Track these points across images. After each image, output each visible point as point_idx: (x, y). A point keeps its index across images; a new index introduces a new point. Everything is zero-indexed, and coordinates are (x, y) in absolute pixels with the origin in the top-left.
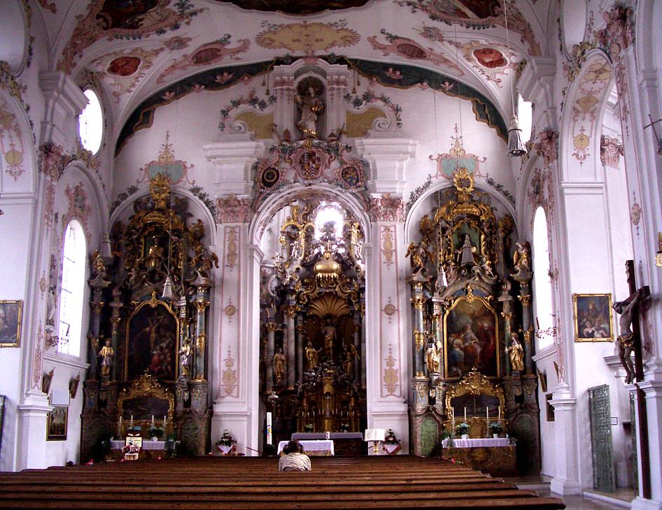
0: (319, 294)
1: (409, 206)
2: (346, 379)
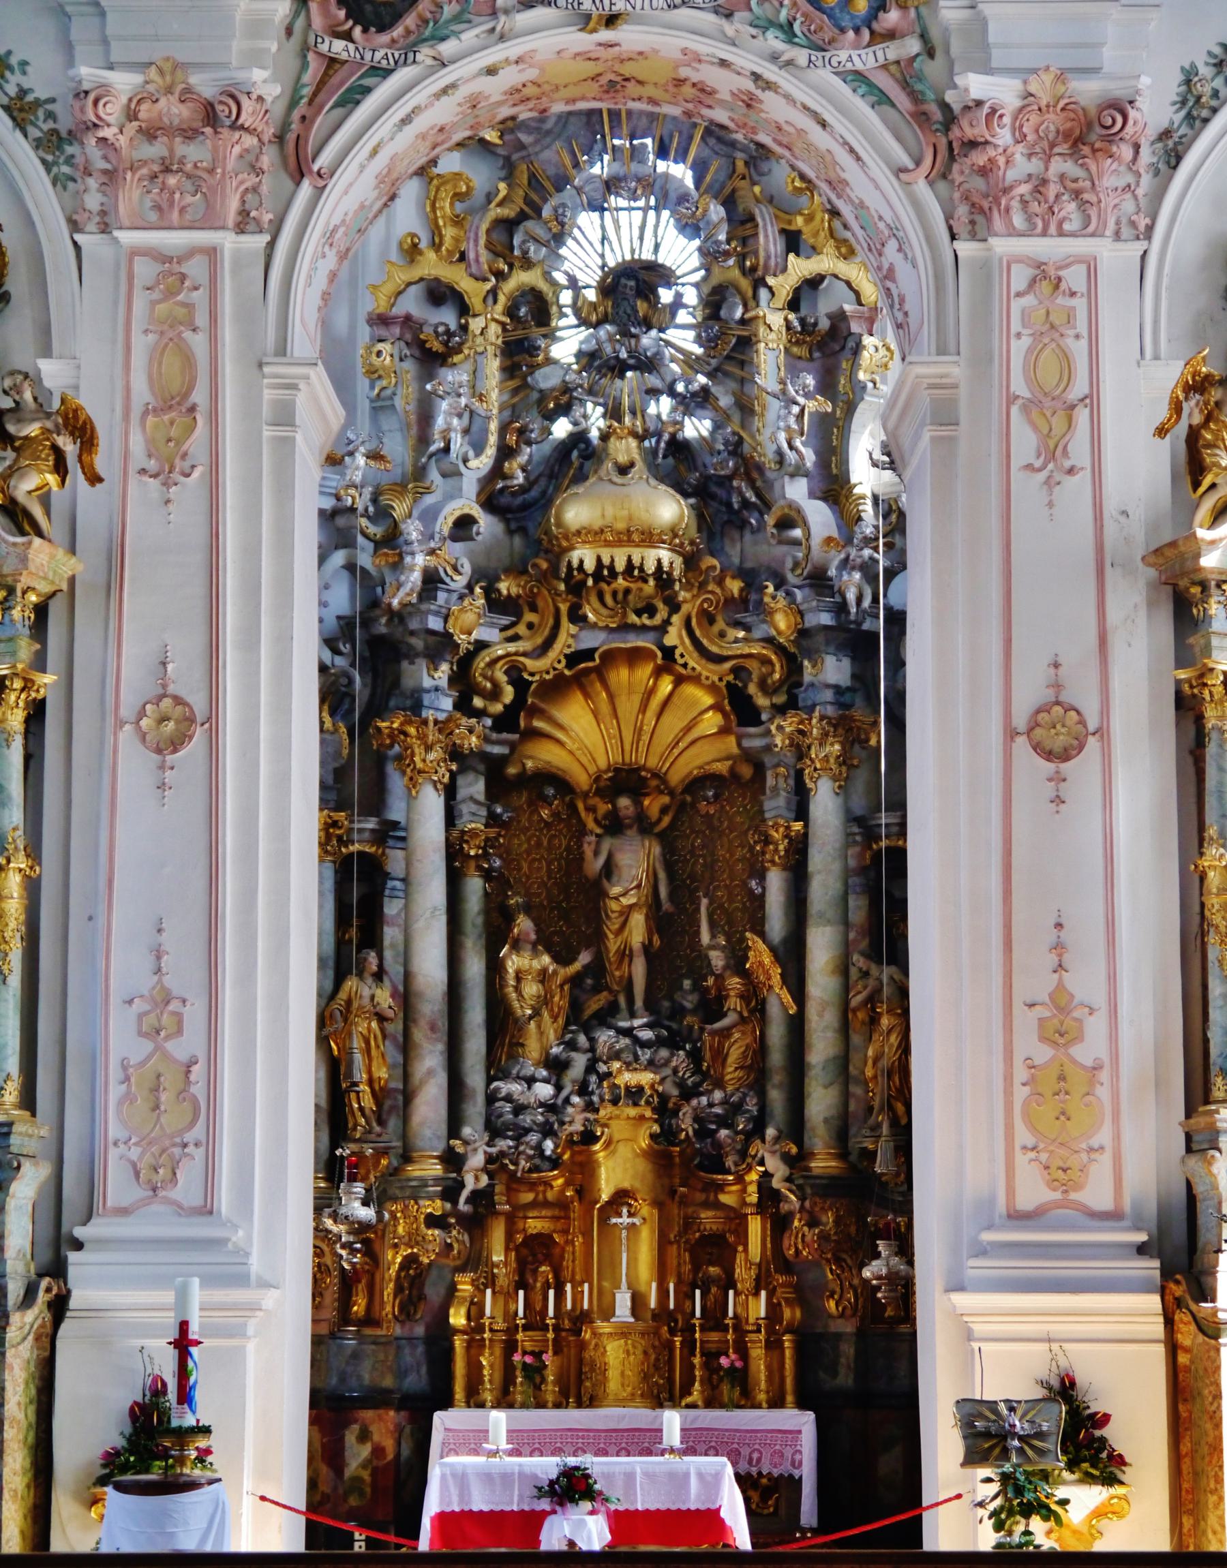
0: (573, 659)
1: (1174, 158)
2: (725, 1121)
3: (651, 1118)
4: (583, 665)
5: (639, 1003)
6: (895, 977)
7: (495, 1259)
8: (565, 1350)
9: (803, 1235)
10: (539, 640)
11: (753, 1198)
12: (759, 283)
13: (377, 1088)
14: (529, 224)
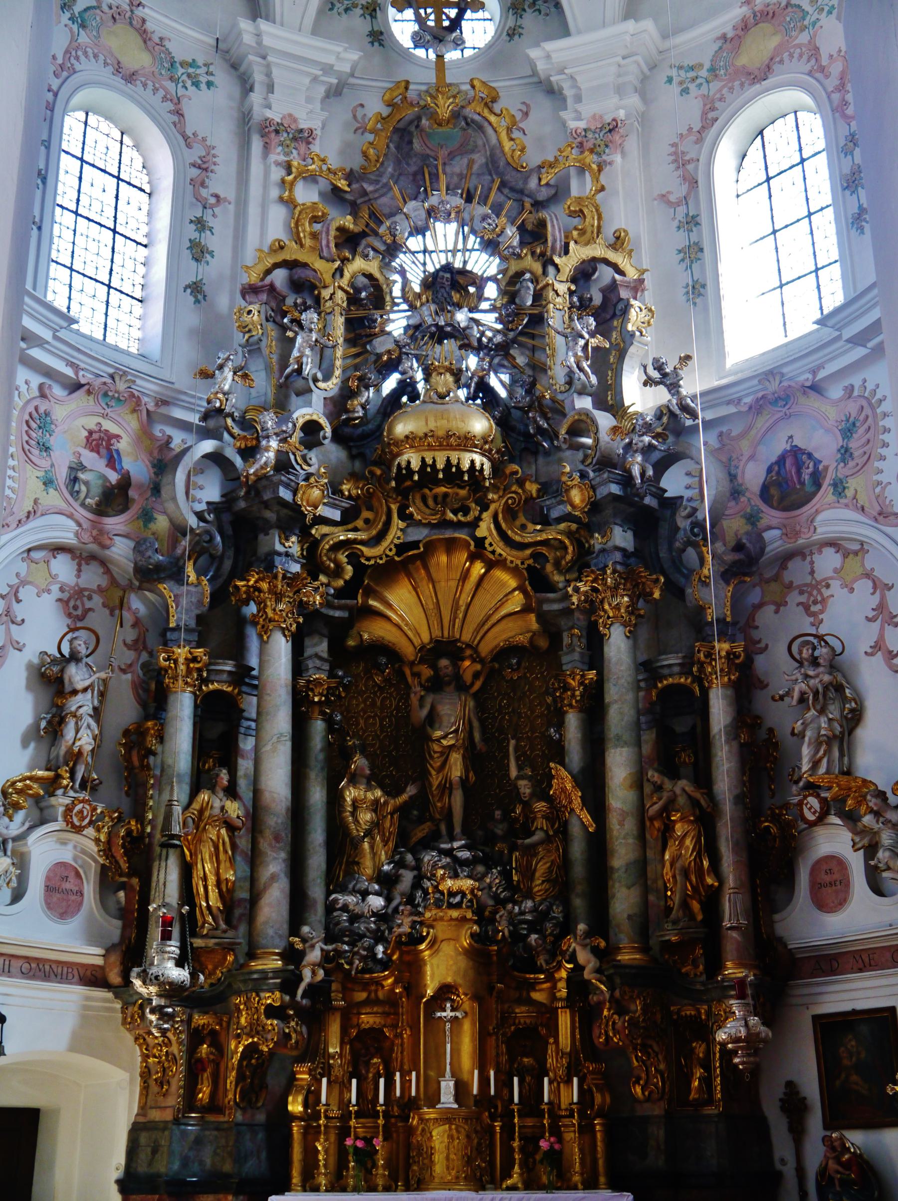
0: (402, 548)
2: (534, 927)
3: (470, 920)
5: (458, 830)
6: (687, 788)
7: (331, 1050)
8: (395, 1135)
9: (614, 1023)
10: (374, 532)
11: (563, 993)
12: (547, 262)
13: (224, 889)
14: (371, 240)
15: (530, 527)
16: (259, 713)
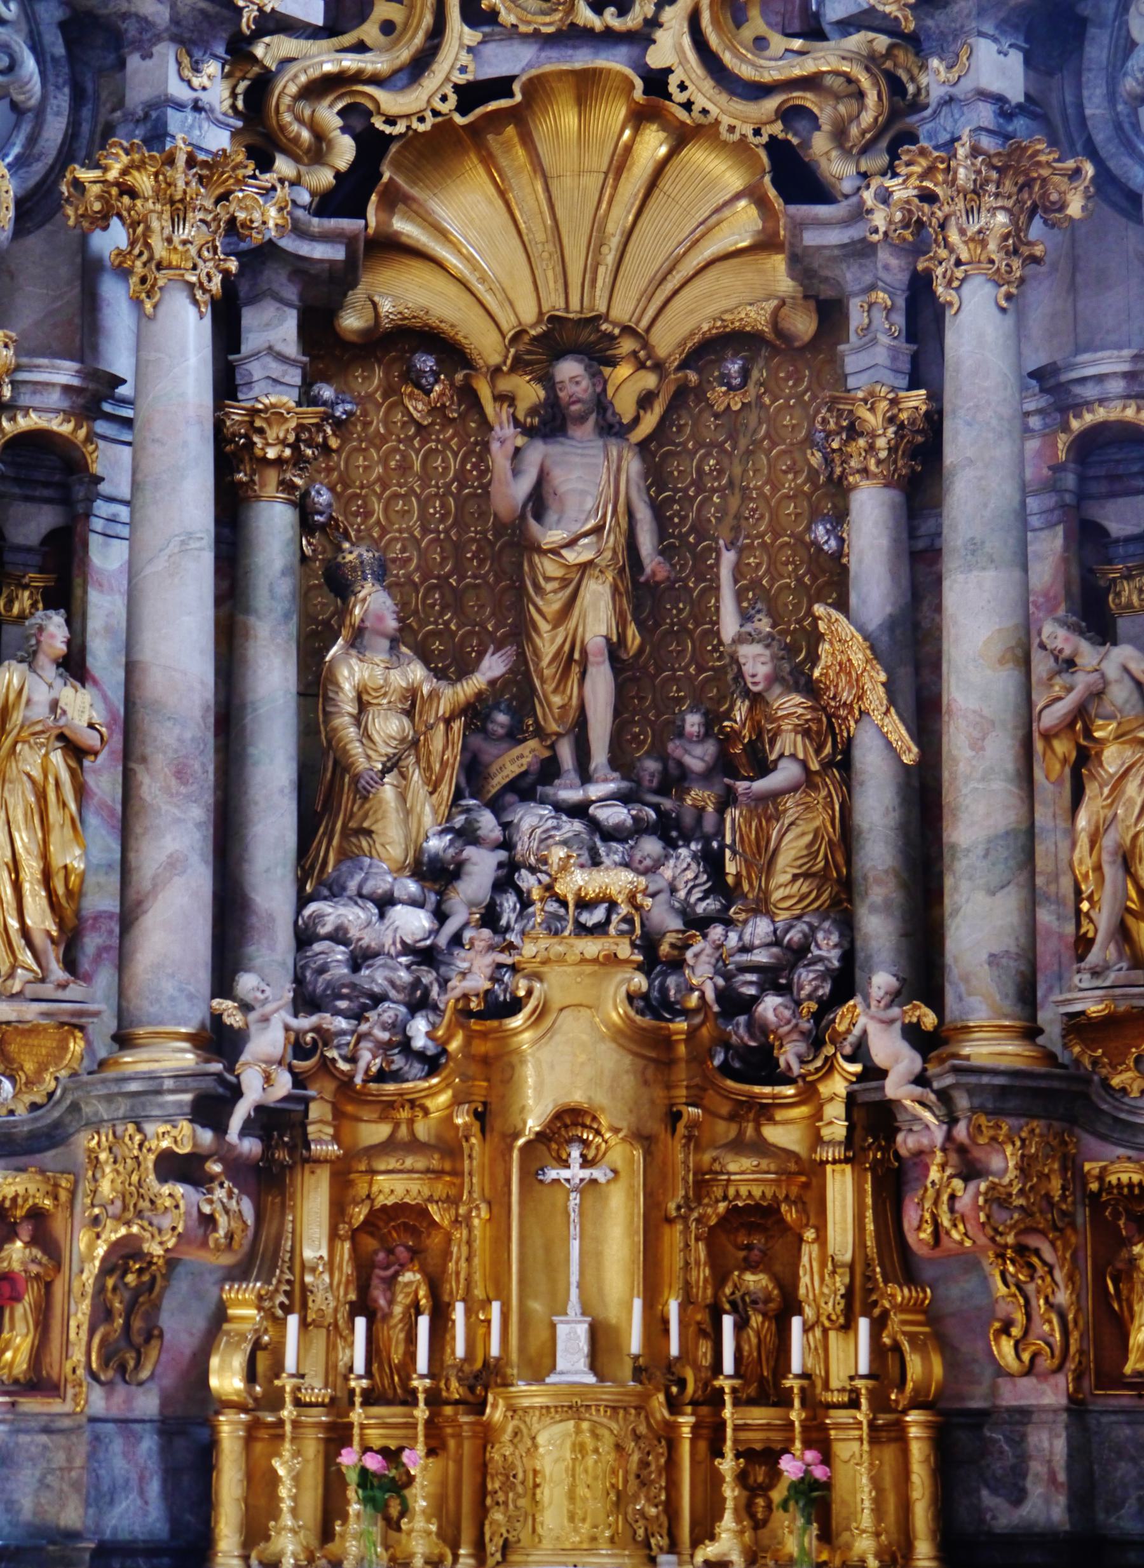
3: (627, 961)
4: (493, 106)
5: (599, 756)
7: (309, 1254)
8: (452, 1443)
9: (953, 1197)
10: (405, 55)
11: (837, 1130)
13: (61, 891)
15: (778, 43)
16: (135, 485)
